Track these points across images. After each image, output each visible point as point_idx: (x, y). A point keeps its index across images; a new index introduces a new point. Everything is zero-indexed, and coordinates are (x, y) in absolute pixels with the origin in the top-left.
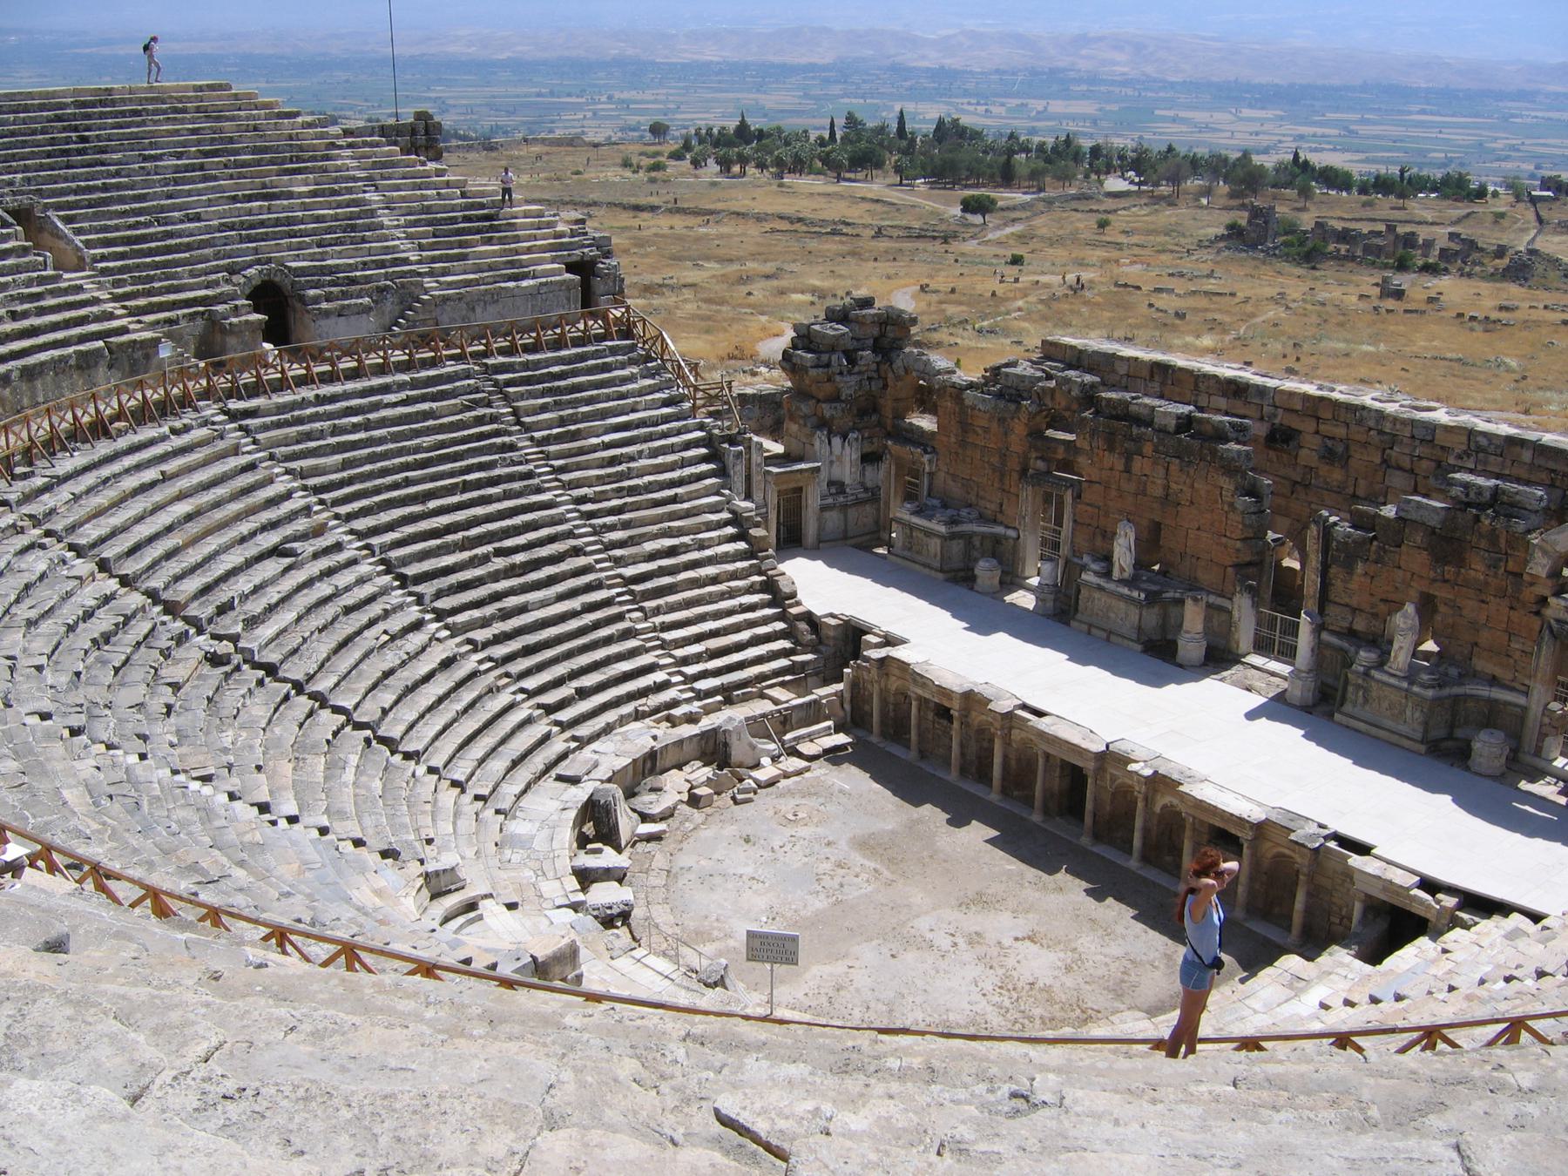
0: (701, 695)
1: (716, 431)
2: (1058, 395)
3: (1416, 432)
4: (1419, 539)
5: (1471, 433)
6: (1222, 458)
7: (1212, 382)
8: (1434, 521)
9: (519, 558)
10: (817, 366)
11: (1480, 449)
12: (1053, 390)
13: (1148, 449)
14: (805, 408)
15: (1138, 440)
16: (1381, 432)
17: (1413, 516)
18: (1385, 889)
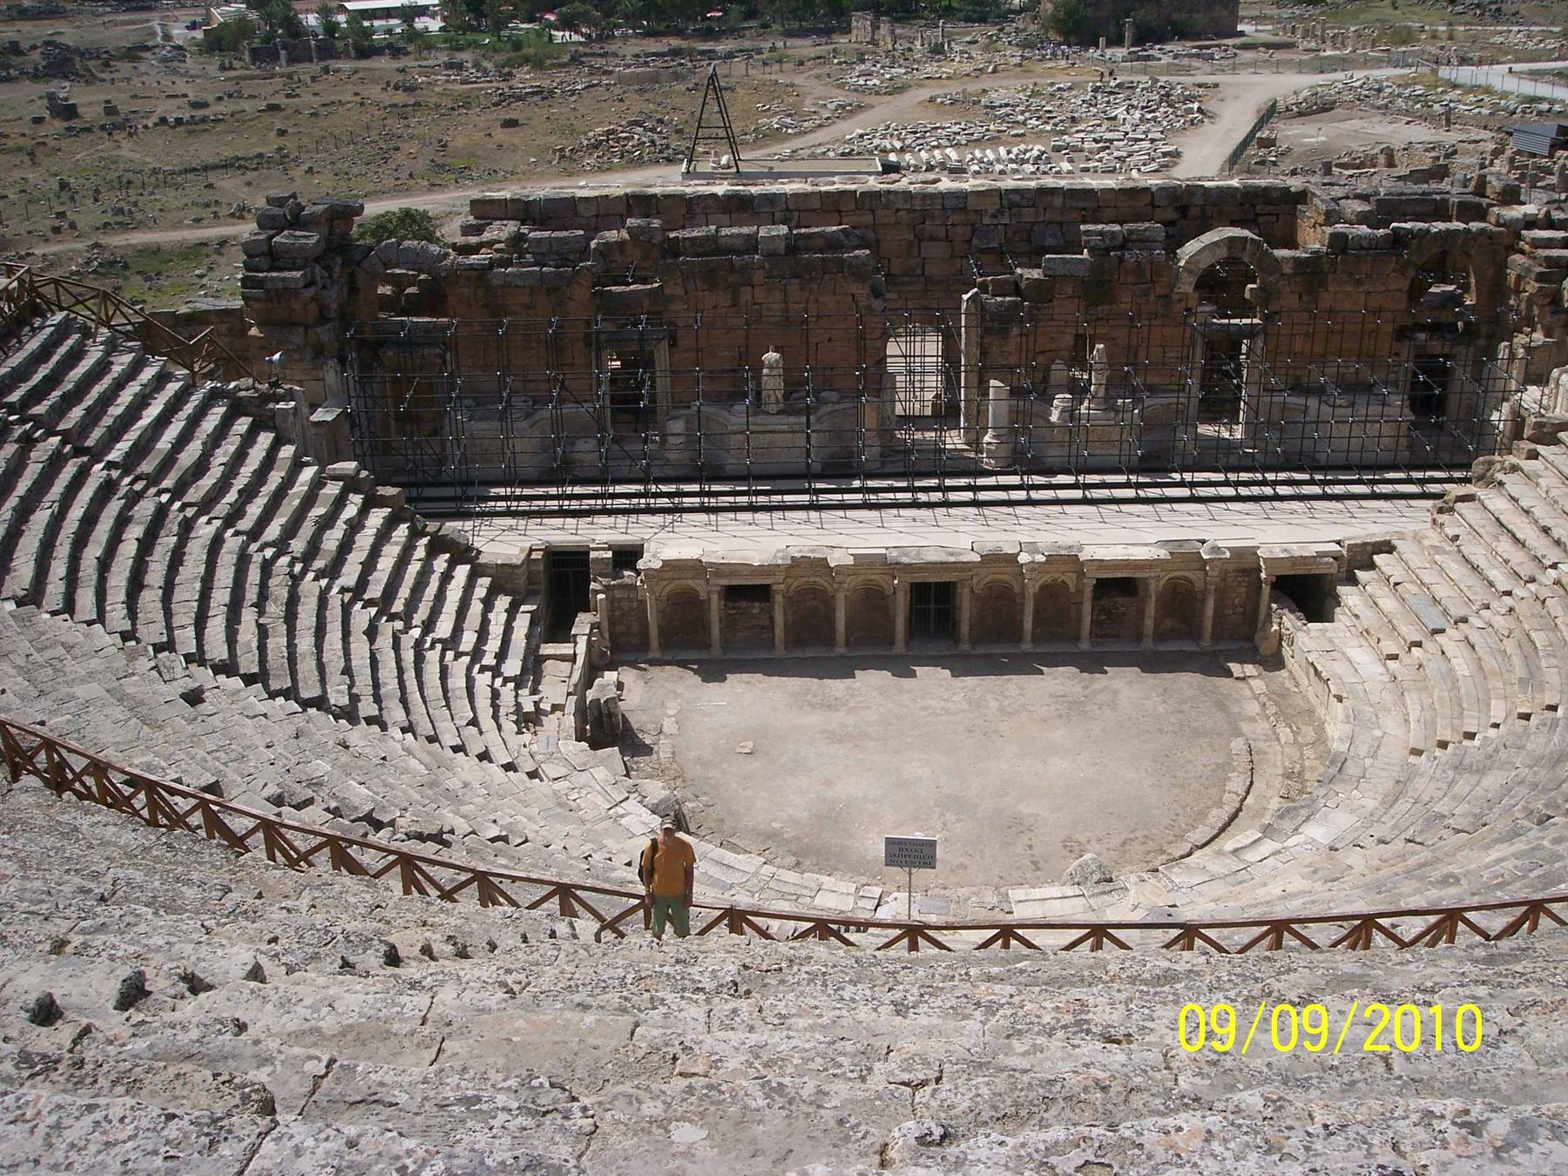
0: (519, 682)
1: (242, 394)
2: (630, 249)
3: (948, 204)
4: (1070, 291)
5: (999, 193)
6: (850, 266)
7: (710, 202)
8: (1082, 271)
9: (275, 609)
10: (307, 286)
11: (1012, 205)
12: (621, 244)
13: (758, 277)
14: (297, 337)
15: (743, 269)
16: (910, 211)
17: (1060, 271)
18: (1294, 565)
